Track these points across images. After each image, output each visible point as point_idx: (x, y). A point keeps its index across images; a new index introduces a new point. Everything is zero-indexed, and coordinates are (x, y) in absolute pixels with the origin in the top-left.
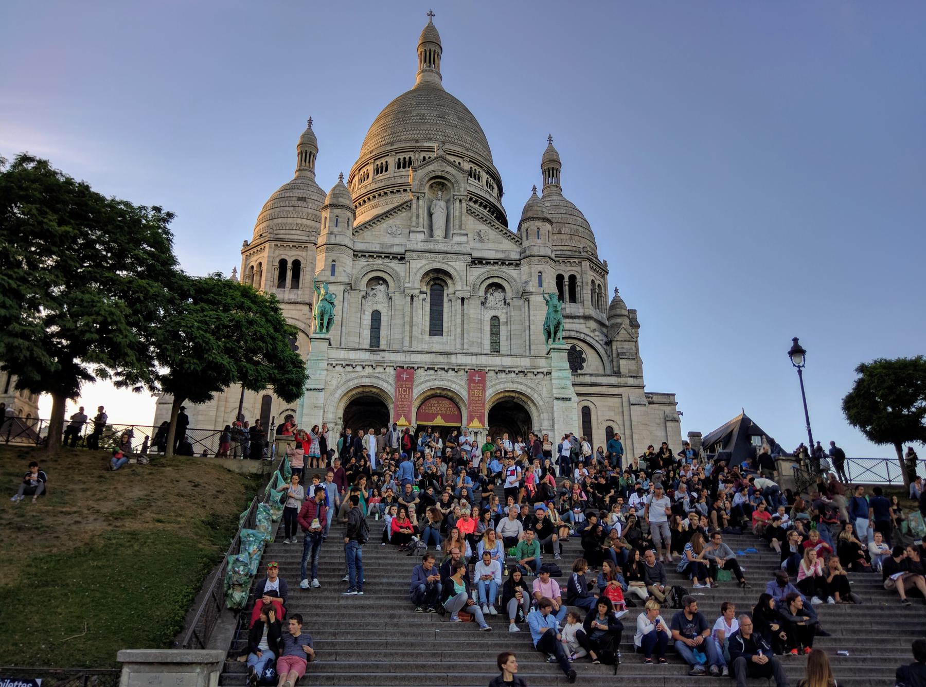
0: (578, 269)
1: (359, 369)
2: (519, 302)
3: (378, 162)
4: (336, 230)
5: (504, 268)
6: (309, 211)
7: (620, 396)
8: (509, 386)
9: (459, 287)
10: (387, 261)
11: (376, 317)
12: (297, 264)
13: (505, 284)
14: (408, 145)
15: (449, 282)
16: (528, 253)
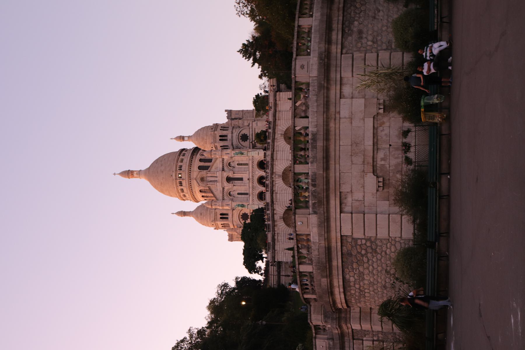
0: (217, 134)
1: (254, 198)
2: (233, 158)
3: (180, 192)
4: (218, 204)
5: (224, 162)
6: (205, 212)
7: (255, 128)
8: (256, 165)
9: (230, 174)
10: (225, 192)
11: (239, 194)
12: (221, 214)
13: (229, 162)
14: (174, 183)
15: (229, 176)
16: (220, 156)
